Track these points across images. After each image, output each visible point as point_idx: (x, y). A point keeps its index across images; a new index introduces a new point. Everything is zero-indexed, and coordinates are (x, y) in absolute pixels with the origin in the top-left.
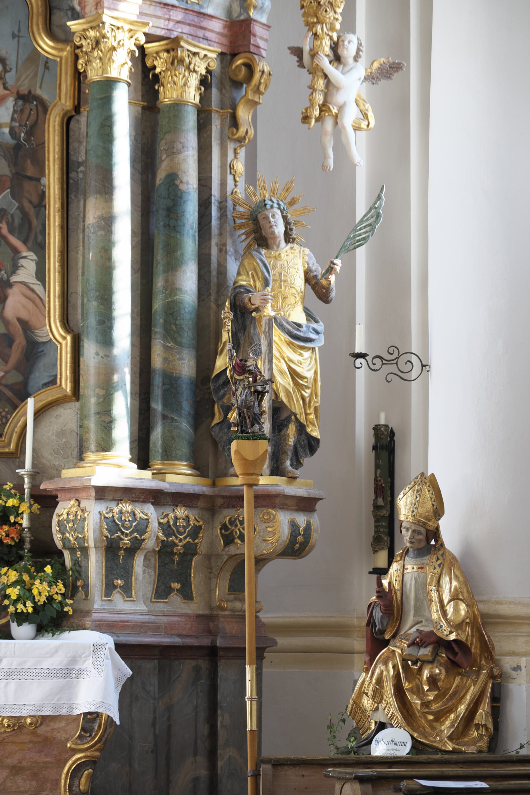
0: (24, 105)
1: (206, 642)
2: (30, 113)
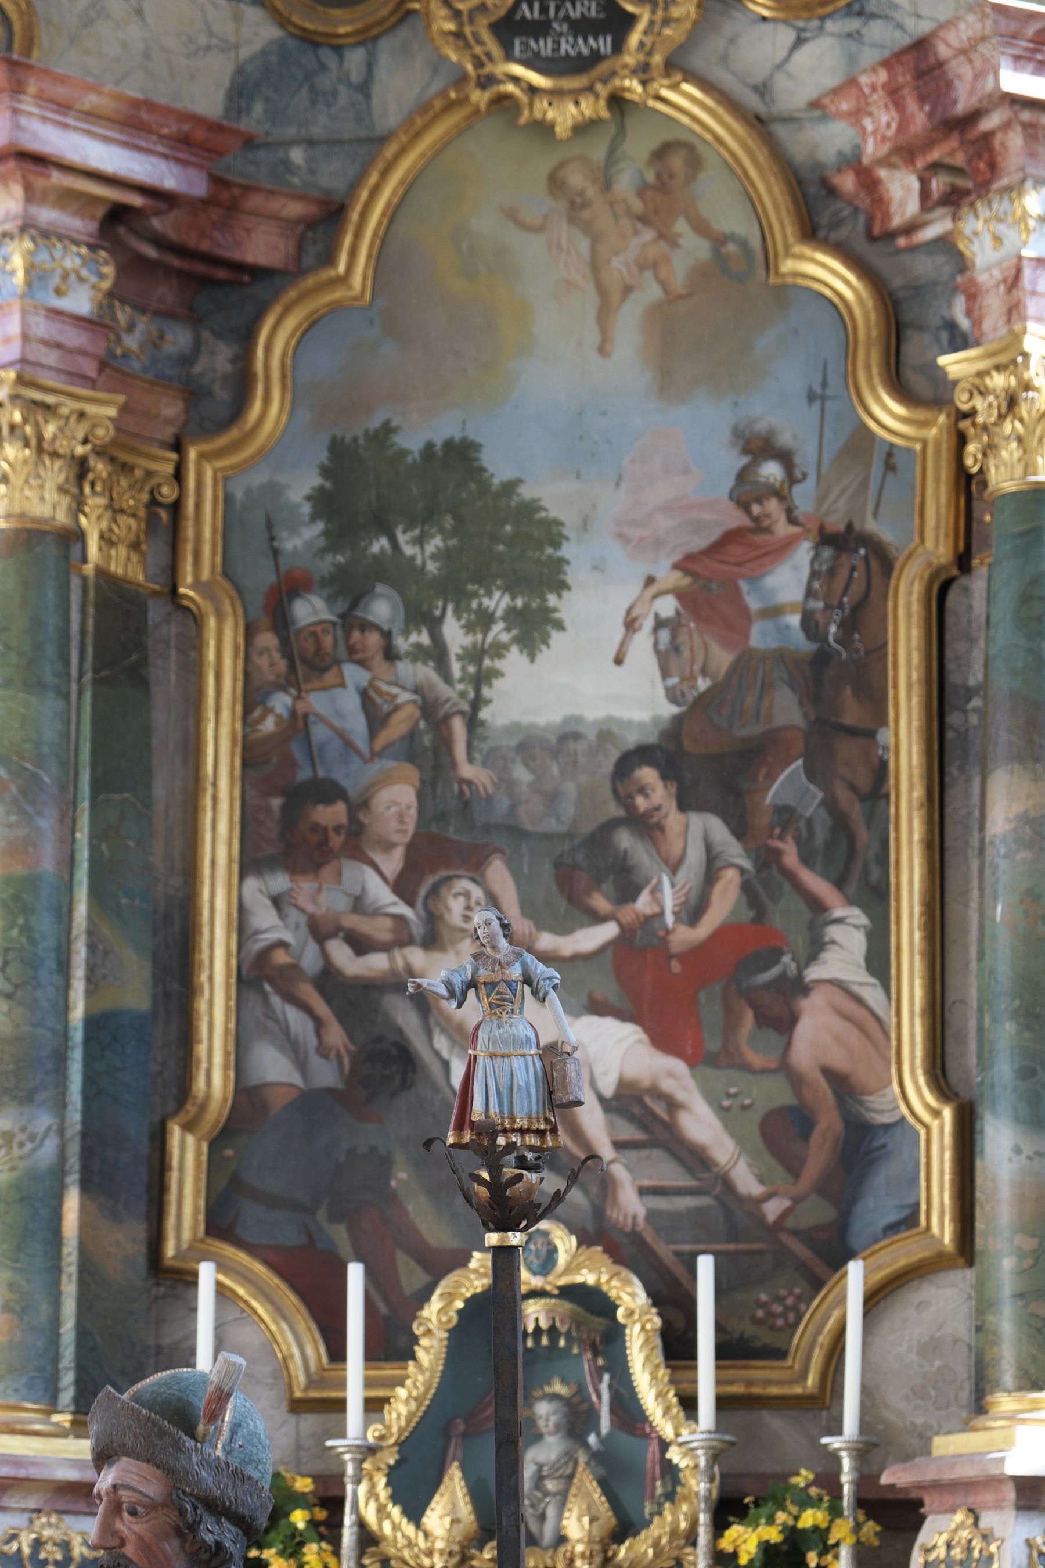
0: (835, 558)
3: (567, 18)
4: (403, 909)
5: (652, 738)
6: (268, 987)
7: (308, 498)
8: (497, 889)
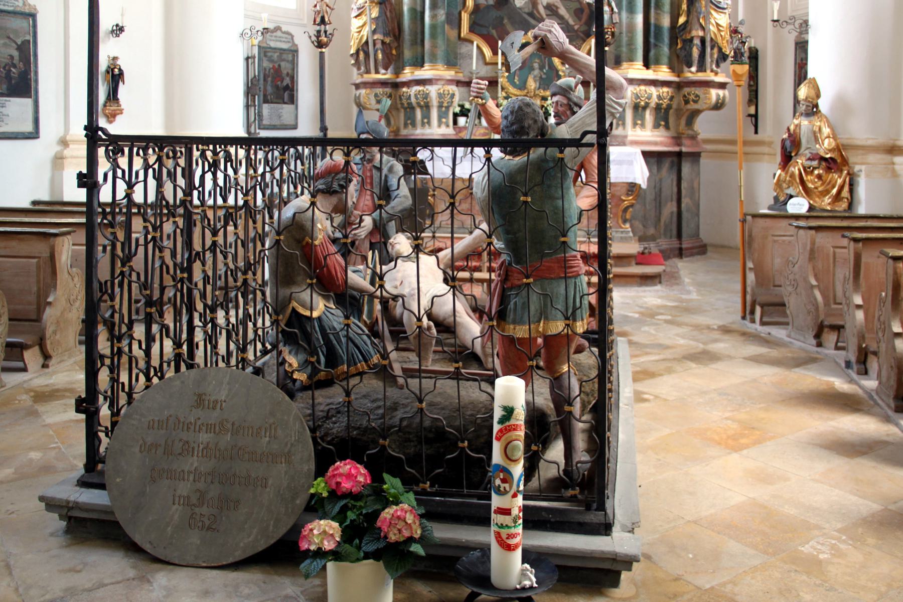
1: (677, 149)
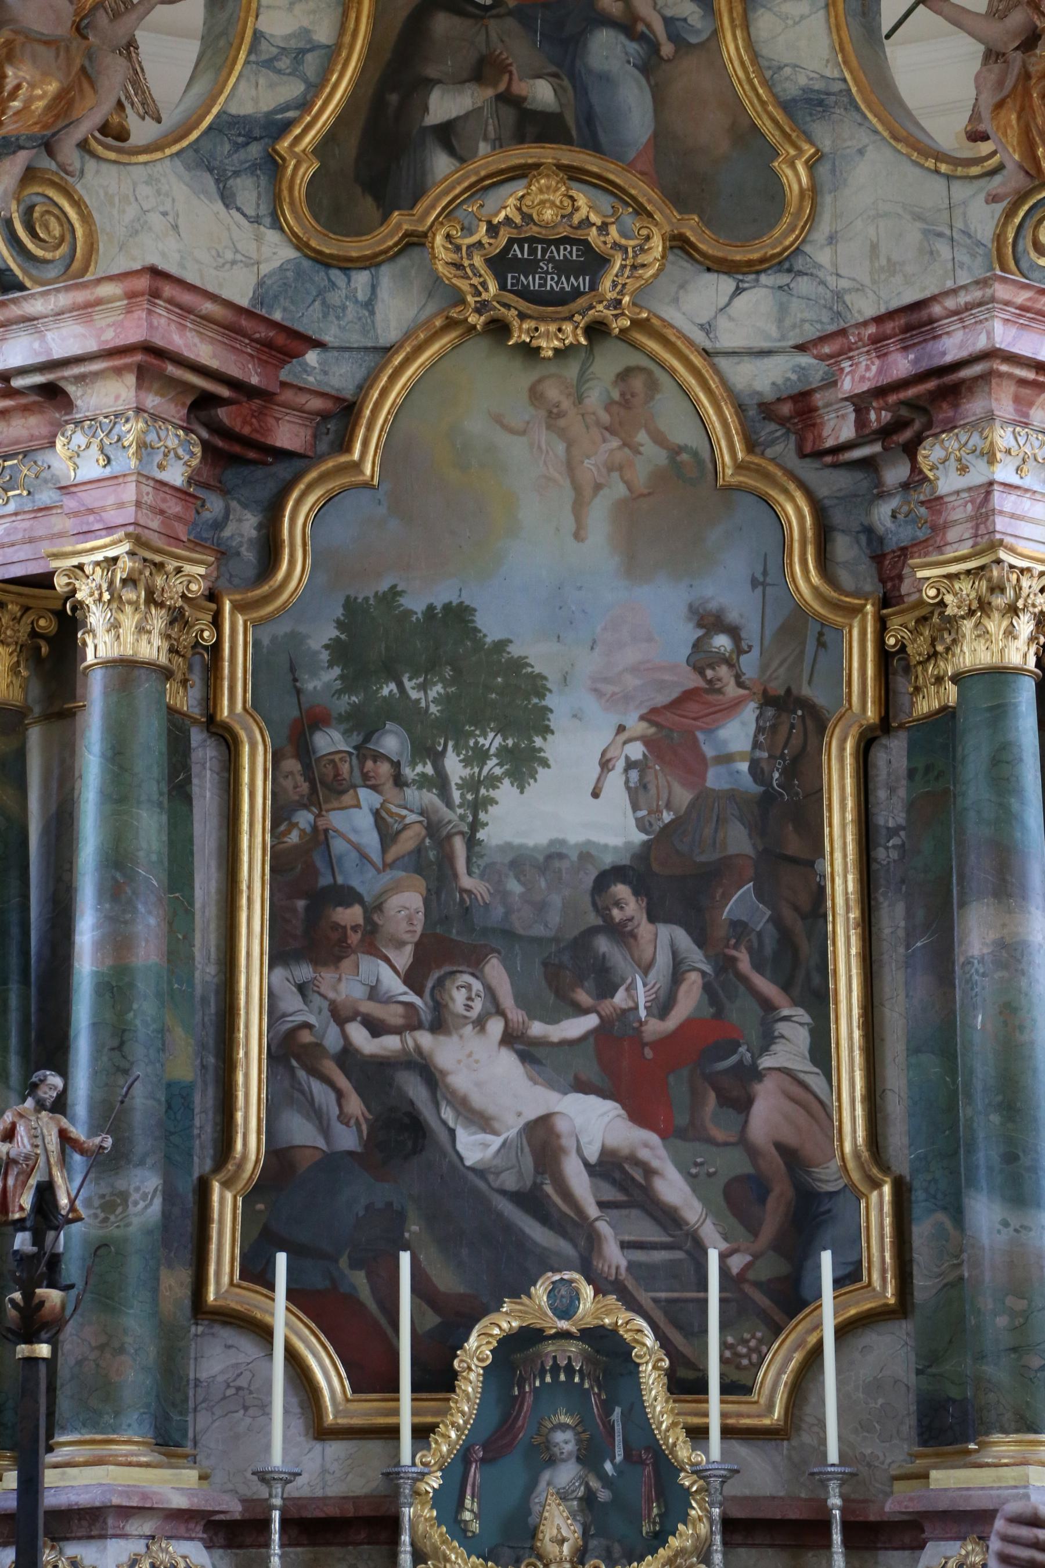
0: (777, 717)
2: (790, 733)
3: (552, 259)
4: (412, 998)
5: (626, 861)
6: (294, 1063)
7: (326, 647)
8: (494, 983)
